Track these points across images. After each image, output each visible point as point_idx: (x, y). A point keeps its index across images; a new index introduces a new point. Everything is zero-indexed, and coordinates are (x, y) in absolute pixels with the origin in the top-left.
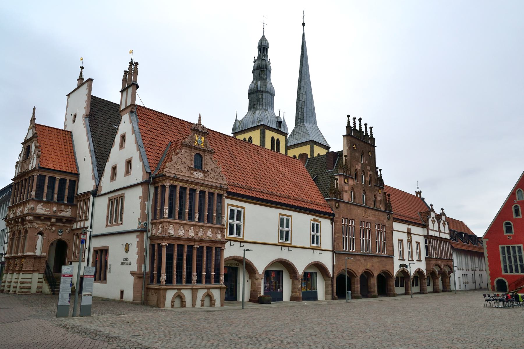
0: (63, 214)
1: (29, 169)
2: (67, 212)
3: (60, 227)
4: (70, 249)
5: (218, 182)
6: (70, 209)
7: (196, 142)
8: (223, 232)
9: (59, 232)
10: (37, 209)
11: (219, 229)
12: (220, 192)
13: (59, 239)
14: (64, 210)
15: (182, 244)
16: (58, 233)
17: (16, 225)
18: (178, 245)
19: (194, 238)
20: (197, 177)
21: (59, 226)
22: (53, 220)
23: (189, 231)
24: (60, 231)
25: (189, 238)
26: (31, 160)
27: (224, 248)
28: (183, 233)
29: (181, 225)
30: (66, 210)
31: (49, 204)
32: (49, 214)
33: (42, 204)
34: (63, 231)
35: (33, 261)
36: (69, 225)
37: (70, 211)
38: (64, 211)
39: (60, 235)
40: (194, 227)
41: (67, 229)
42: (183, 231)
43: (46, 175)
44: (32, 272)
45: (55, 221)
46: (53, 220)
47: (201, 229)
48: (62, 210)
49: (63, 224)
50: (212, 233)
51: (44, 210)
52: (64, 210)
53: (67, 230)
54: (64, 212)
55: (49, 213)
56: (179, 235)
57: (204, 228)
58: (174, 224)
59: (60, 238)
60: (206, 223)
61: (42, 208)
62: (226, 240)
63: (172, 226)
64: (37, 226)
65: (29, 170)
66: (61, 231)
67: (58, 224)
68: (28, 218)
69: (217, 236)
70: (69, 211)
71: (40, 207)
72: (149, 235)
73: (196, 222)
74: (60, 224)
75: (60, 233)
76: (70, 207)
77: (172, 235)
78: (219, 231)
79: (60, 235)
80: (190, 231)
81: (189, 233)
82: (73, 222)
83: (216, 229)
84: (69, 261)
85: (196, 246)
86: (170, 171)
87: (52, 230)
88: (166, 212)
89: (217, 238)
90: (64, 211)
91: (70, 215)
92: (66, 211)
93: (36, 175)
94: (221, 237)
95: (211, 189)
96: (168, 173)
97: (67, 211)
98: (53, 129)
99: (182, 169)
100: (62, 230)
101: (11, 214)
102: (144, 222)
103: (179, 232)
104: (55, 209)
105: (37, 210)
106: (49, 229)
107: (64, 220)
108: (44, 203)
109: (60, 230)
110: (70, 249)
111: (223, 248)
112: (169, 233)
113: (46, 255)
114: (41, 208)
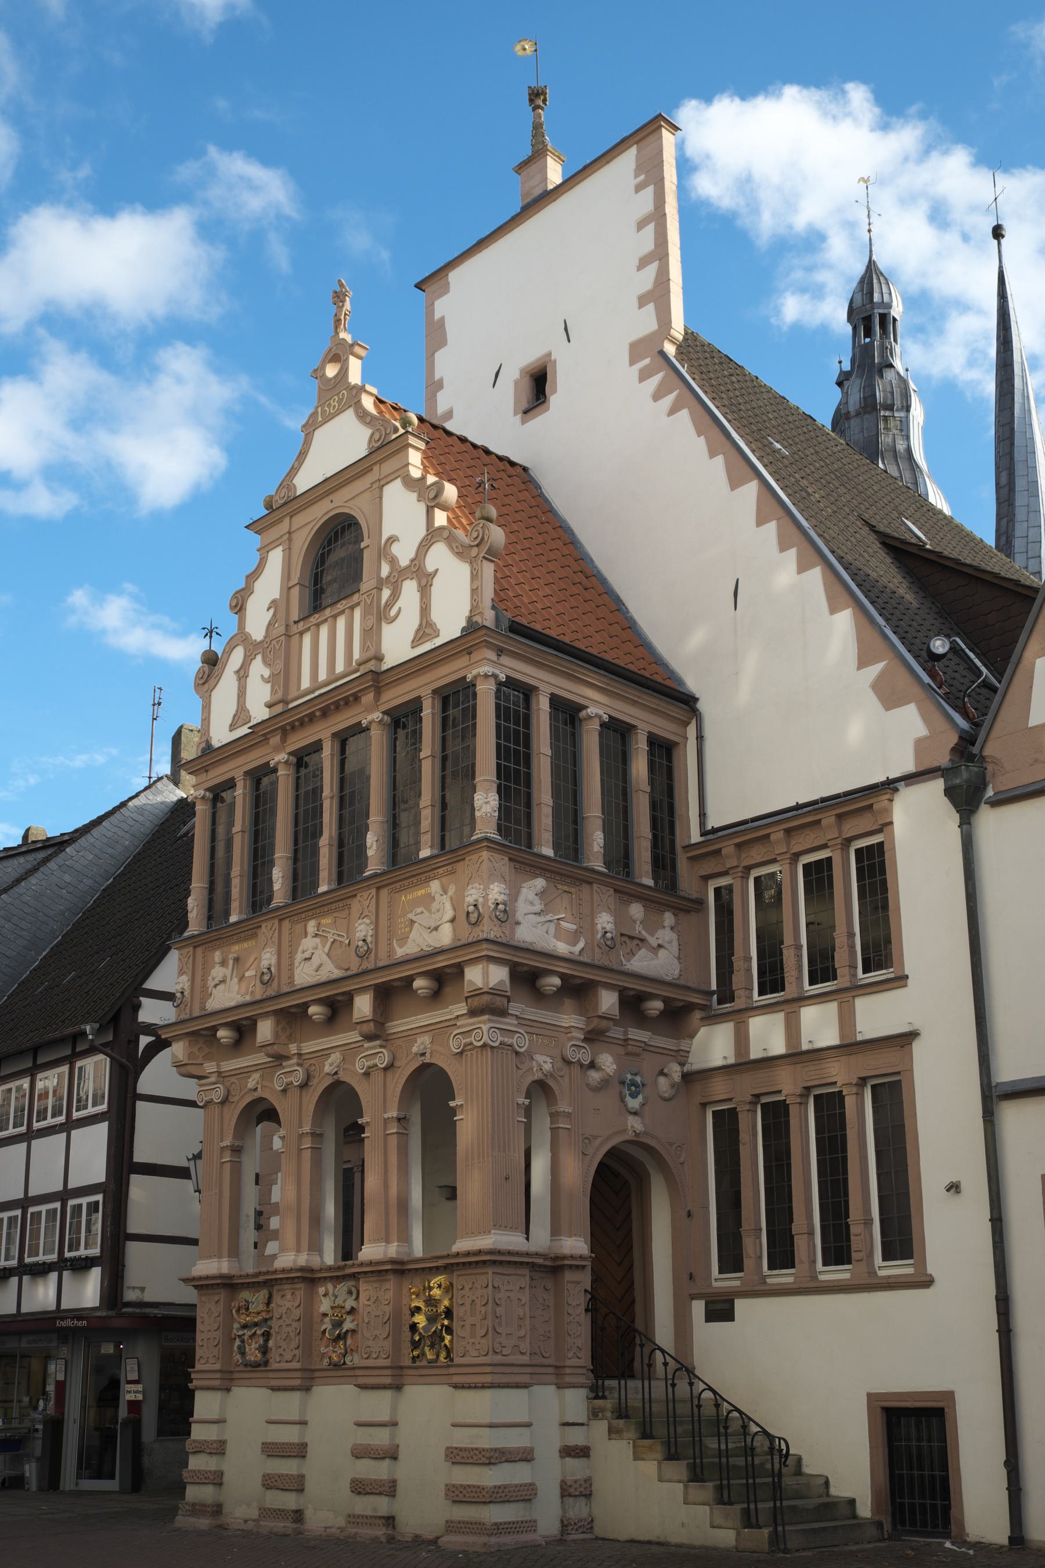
1: (380, 658)
2: (662, 953)
3: (627, 1054)
4: (689, 1214)
10: (519, 916)
13: (630, 1136)
14: (644, 933)
16: (622, 1100)
17: (293, 1049)
21: (621, 1051)
22: (608, 1001)
26: (395, 596)
30: (652, 935)
31: (573, 890)
33: (540, 883)
34: (643, 1085)
35: (525, 1298)
37: (675, 943)
41: (661, 1073)
44: (526, 1379)
45: (616, 1012)
48: (636, 933)
51: (552, 928)
52: (644, 933)
53: (662, 1080)
59: (637, 1134)
61: (539, 914)
64: (521, 1042)
65: (385, 667)
66: (636, 1086)
67: (616, 1032)
68: (486, 974)
70: (670, 942)
71: (532, 903)
82: (697, 1015)
84: (693, 1297)
87: (595, 1076)
92: (653, 941)
93: (492, 681)
97: (660, 946)
100: (638, 1079)
101: (223, 981)
104: (605, 921)
105: (518, 923)
106: (582, 1066)
108: (546, 878)
109: (629, 1077)
110: (689, 1214)
114: (538, 907)
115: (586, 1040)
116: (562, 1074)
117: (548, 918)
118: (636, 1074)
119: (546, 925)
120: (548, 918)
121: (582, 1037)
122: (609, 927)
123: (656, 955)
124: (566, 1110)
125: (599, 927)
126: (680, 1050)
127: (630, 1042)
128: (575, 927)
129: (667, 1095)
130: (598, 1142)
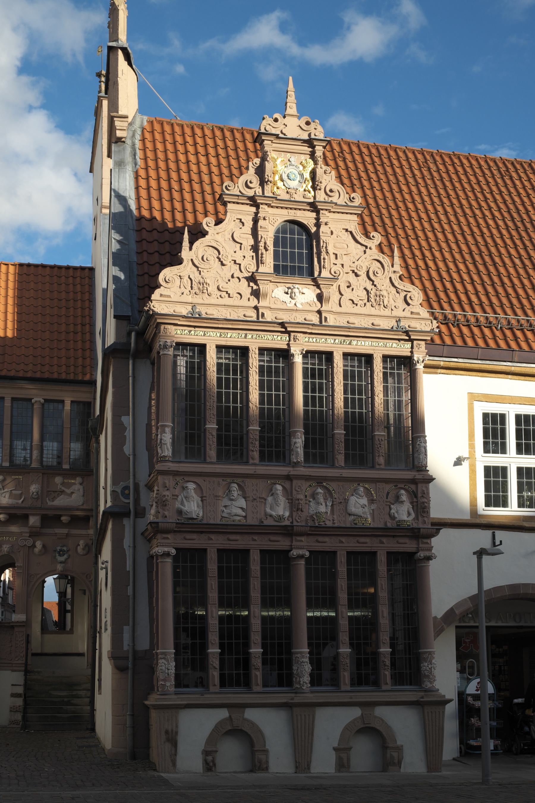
0: (61, 501)
2: (74, 496)
5: (387, 312)
6: (81, 484)
7: (280, 184)
8: (420, 495)
9: (59, 553)
11: (400, 486)
12: (403, 349)
14: (63, 488)
15: (241, 547)
18: (263, 552)
19: (287, 523)
20: (291, 305)
22: (33, 520)
23: (265, 500)
24: (61, 550)
25: (266, 523)
27: (427, 554)
28: (242, 508)
29: (229, 480)
32: (23, 505)
36: (83, 532)
37: (81, 490)
38: (63, 492)
39: (61, 563)
40: (287, 485)
42: (242, 503)
43: (3, 396)
45: (38, 524)
46: (33, 520)
47: (320, 490)
49: (65, 531)
50: (371, 501)
52: (63, 488)
54: (62, 496)
55: (22, 502)
56: (224, 515)
57: (332, 486)
58: (200, 480)
60: (342, 468)
62: (433, 524)
63: (191, 486)
66: (64, 551)
69: (392, 511)
70: (79, 490)
72: (142, 525)
73: (297, 464)
74: (58, 531)
75: (60, 555)
76: (79, 480)
77: (193, 519)
78: (403, 492)
79: (61, 563)
80: (270, 499)
81: (268, 506)
83: (388, 487)
85: (295, 553)
86: (169, 296)
88: (161, 439)
89: (393, 518)
90: (63, 492)
91: (81, 503)
92: (68, 491)
94: (413, 515)
95: (354, 343)
96: (163, 305)
97: (72, 493)
98: (40, 267)
99: (222, 285)
100: (65, 548)
102: (122, 484)
103: (225, 506)
104: (34, 488)
107: (64, 519)
109: (58, 548)
111: (422, 554)
112: (180, 512)
113: (25, 620)
115: (30, 536)
116: (19, 551)
117: (5, 491)
118: (63, 546)
119: (4, 494)
120: (5, 491)
121: (28, 535)
122: (34, 490)
123: (71, 497)
124: (19, 565)
125: (31, 491)
126: (89, 534)
127: (57, 534)
128: (21, 492)
129: (82, 553)
130: (38, 576)
